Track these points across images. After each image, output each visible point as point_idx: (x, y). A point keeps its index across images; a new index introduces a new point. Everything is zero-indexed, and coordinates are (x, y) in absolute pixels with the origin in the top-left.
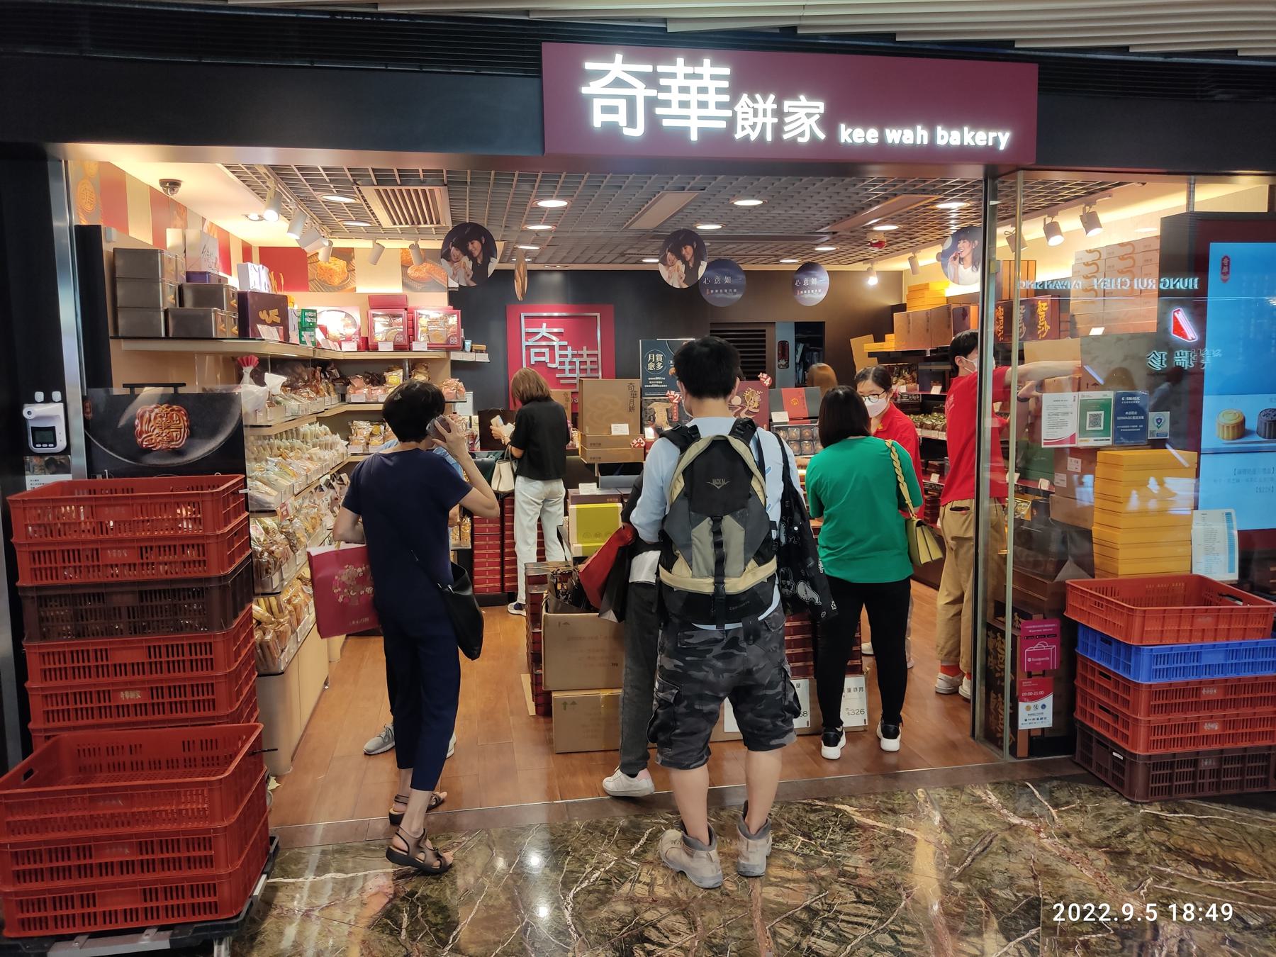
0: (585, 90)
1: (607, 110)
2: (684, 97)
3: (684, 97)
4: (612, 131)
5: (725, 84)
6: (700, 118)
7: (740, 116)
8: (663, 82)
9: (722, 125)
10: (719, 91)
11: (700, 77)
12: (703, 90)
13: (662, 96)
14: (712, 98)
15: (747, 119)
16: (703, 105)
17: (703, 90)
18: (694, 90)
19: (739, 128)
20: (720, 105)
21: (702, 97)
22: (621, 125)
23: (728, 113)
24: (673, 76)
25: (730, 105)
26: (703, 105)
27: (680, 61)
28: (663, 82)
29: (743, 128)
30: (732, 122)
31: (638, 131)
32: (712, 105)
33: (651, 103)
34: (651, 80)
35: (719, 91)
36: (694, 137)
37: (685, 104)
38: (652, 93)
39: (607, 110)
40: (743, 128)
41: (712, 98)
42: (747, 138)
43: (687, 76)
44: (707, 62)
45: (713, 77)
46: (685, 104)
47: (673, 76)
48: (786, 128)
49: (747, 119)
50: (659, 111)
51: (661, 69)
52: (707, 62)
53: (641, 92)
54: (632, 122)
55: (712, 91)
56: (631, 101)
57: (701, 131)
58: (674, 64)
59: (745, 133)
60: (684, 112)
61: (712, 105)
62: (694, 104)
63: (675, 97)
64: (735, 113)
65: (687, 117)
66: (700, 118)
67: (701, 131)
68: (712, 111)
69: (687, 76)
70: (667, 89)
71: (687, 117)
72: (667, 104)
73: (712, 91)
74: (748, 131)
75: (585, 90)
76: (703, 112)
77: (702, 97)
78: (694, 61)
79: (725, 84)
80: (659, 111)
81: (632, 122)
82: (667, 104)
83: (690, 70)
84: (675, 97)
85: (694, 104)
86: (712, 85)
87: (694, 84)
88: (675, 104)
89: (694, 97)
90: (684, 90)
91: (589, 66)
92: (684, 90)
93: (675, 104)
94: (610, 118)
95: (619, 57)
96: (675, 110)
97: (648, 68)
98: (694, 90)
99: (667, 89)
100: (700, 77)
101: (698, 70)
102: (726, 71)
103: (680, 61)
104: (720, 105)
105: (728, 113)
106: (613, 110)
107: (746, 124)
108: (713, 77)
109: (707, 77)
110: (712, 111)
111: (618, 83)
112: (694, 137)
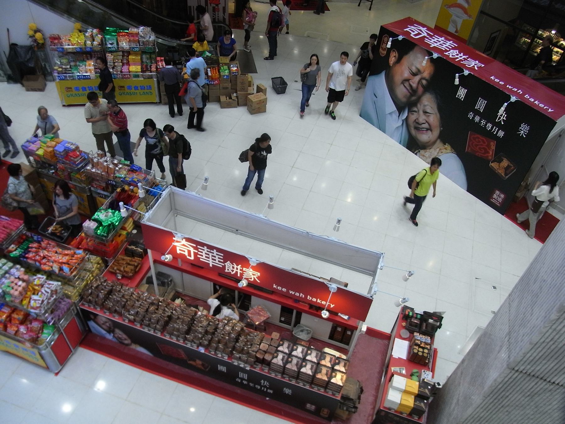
7: (227, 266)
8: (199, 250)
11: (213, 253)
24: (204, 250)
28: (199, 250)
29: (228, 270)
30: (224, 267)
31: (192, 258)
38: (197, 251)
40: (228, 270)
43: (207, 251)
53: (192, 250)
57: (213, 265)
64: (225, 265)
67: (213, 265)
68: (217, 262)
80: (198, 256)
86: (217, 256)
96: (204, 257)
97: (195, 245)
99: (202, 252)
100: (213, 253)
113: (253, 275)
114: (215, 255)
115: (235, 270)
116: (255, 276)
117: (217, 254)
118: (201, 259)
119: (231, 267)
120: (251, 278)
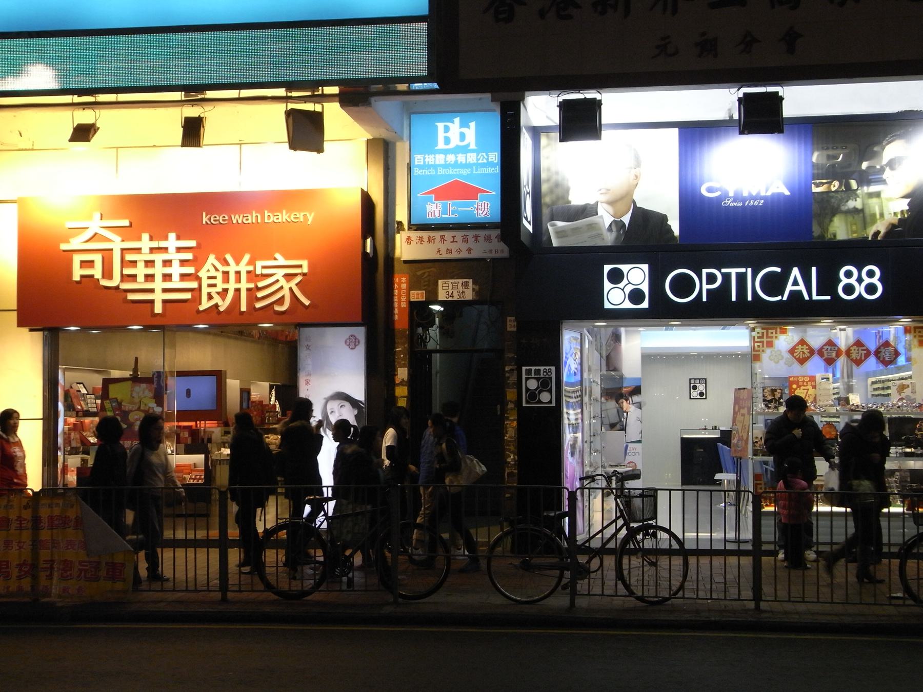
9: (187, 296)
10: (183, 263)
11: (165, 250)
12: (168, 263)
14: (176, 270)
15: (214, 285)
17: (168, 263)
18: (159, 264)
19: (204, 297)
20: (184, 277)
21: (167, 270)
29: (210, 297)
32: (176, 277)
35: (183, 263)
36: (158, 309)
37: (150, 278)
40: (210, 297)
41: (176, 270)
42: (216, 306)
43: (152, 250)
44: (172, 236)
45: (179, 250)
48: (260, 294)
49: (214, 285)
55: (176, 264)
59: (212, 303)
60: (148, 286)
61: (176, 277)
62: (158, 278)
65: (152, 291)
66: (165, 291)
67: (165, 302)
68: (176, 283)
69: (152, 250)
71: (152, 291)
73: (176, 264)
74: (217, 299)
79: (189, 256)
85: (158, 278)
86: (176, 257)
87: (159, 258)
88: (141, 278)
90: (149, 263)
93: (141, 278)
96: (141, 284)
98: (159, 264)
99: (134, 263)
100: (165, 250)
102: (192, 243)
104: (184, 277)
107: (213, 290)
108: (179, 250)
109: (172, 250)
112: (158, 309)
113: (289, 277)
115: (232, 286)
116: (293, 284)
118: (131, 297)
119: (219, 281)
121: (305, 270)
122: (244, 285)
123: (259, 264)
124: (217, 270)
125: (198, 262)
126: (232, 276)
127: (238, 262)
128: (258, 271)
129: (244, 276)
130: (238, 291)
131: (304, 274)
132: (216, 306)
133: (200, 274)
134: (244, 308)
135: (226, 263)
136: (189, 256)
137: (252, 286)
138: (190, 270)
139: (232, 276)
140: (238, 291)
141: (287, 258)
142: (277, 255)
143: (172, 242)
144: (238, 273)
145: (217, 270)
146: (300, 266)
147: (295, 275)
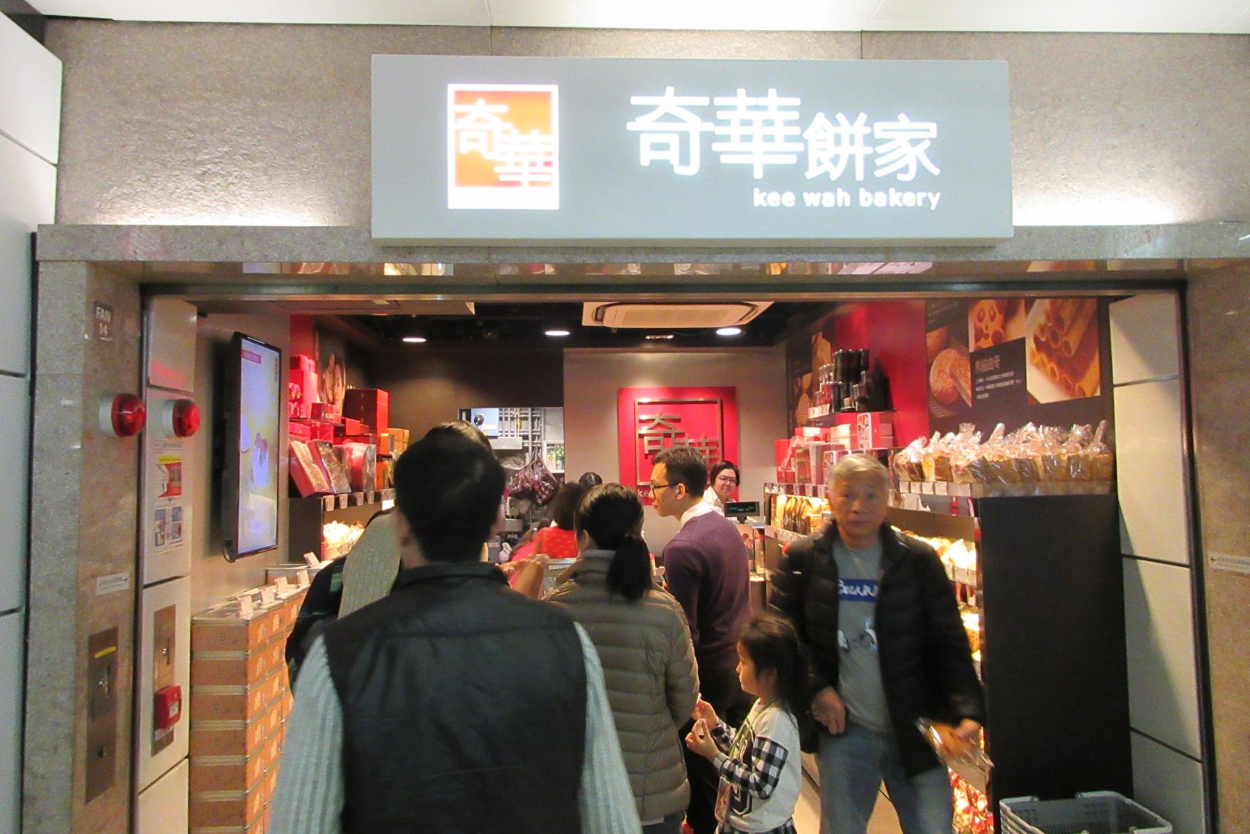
0: (630, 126)
1: (655, 147)
2: (747, 130)
3: (747, 130)
4: (662, 168)
5: (795, 115)
6: (765, 153)
9: (792, 160)
10: (789, 123)
11: (765, 108)
12: (768, 123)
13: (720, 131)
14: (780, 131)
16: (769, 139)
17: (768, 123)
20: (789, 139)
21: (769, 131)
22: (671, 163)
23: (799, 147)
24: (733, 108)
25: (799, 138)
26: (769, 139)
27: (741, 92)
28: (721, 115)
29: (819, 163)
30: (803, 158)
31: (693, 169)
32: (779, 139)
33: (708, 139)
34: (708, 113)
35: (789, 123)
37: (747, 138)
39: (655, 147)
40: (819, 163)
41: (780, 131)
42: (827, 174)
43: (750, 108)
44: (772, 92)
46: (747, 138)
47: (733, 108)
50: (716, 147)
51: (719, 101)
52: (772, 92)
53: (695, 126)
54: (685, 159)
56: (684, 138)
58: (735, 95)
61: (779, 139)
63: (735, 131)
68: (779, 144)
69: (750, 108)
70: (726, 123)
72: (726, 139)
74: (827, 166)
75: (630, 126)
76: (769, 146)
77: (769, 131)
78: (757, 89)
80: (716, 147)
81: (685, 159)
82: (726, 139)
83: (754, 101)
84: (735, 131)
87: (757, 116)
89: (757, 131)
90: (746, 123)
91: (635, 100)
92: (746, 123)
94: (660, 155)
95: (670, 90)
96: (735, 144)
97: (704, 101)
99: (726, 123)
100: (765, 108)
101: (760, 101)
103: (741, 92)
104: (789, 139)
105: (799, 147)
106: (664, 147)
108: (782, 108)
110: (779, 144)
111: (668, 117)
112: (758, 174)
113: (915, 142)
114: (772, 114)
115: (845, 151)
117: (782, 108)
118: (724, 159)
120: (905, 170)
121: (934, 135)
122: (861, 151)
123: (879, 126)
124: (826, 131)
125: (805, 121)
126: (845, 140)
127: (852, 122)
128: (878, 135)
129: (859, 140)
130: (852, 159)
131: (930, 139)
132: (827, 174)
133: (805, 135)
134: (860, 176)
135: (836, 123)
136: (795, 115)
137: (869, 150)
138: (796, 130)
139: (845, 140)
140: (852, 159)
141: (912, 118)
142: (902, 117)
143: (772, 98)
144: (852, 137)
145: (826, 131)
146: (928, 130)
147: (923, 140)
